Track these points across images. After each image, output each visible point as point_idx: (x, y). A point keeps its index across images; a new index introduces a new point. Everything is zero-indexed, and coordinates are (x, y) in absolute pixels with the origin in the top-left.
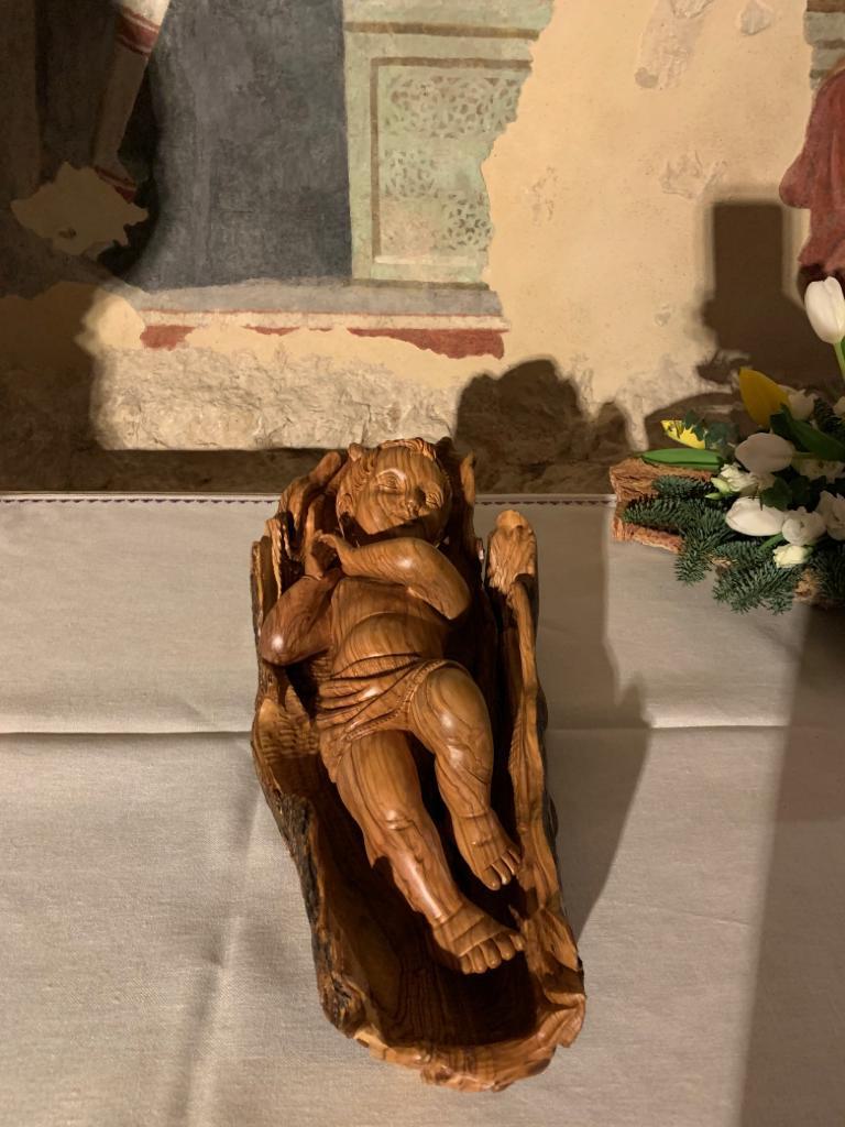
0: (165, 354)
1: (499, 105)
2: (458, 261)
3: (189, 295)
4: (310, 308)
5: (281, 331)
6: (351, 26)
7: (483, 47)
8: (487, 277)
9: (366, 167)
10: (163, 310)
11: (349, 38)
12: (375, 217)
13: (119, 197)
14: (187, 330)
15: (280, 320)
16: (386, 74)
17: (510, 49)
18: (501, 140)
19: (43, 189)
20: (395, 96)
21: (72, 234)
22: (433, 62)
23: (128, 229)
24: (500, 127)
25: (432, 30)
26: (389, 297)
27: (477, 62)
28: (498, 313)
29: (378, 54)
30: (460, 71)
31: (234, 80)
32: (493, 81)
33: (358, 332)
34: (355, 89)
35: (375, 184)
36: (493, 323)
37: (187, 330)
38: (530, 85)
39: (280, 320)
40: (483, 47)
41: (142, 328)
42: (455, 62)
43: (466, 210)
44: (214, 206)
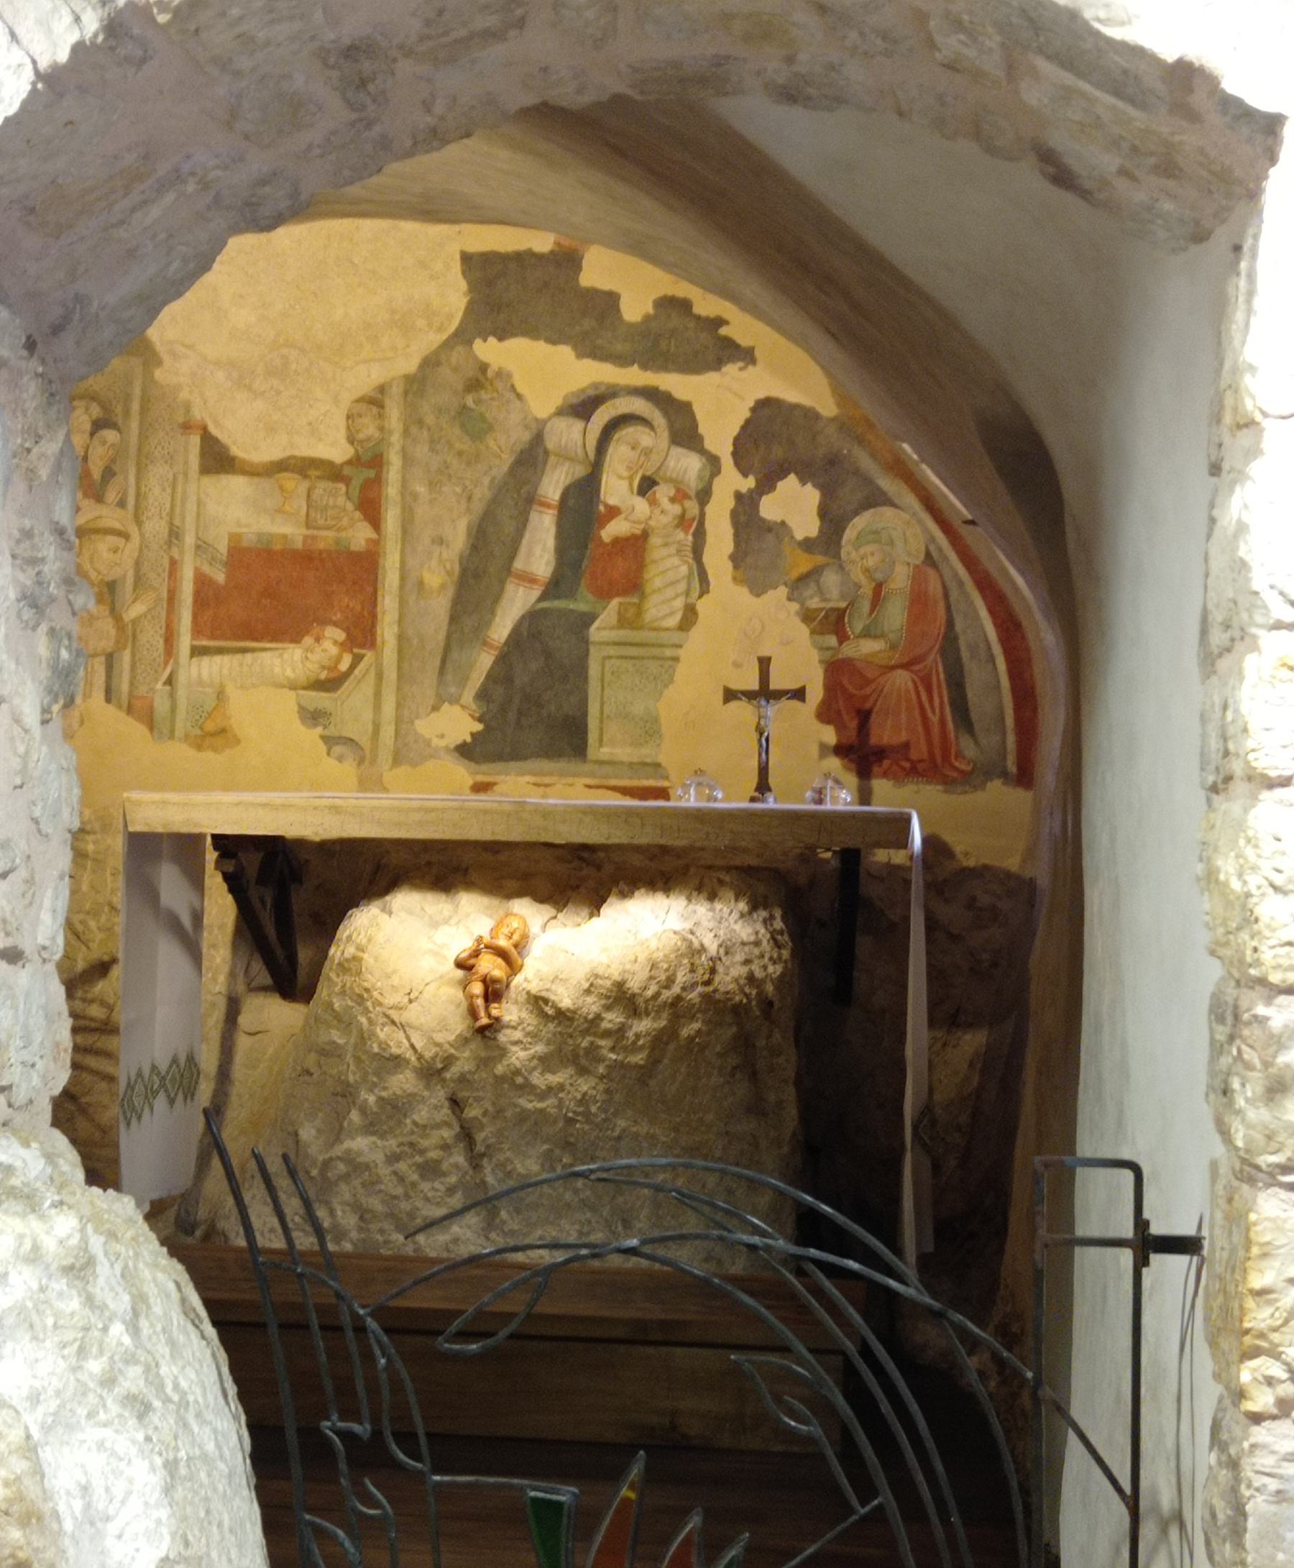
0: (482, 797)
3: (499, 766)
4: (562, 774)
5: (546, 786)
6: (592, 643)
7: (656, 651)
8: (661, 759)
9: (597, 705)
10: (484, 774)
11: (592, 650)
12: (601, 729)
13: (470, 719)
14: (495, 784)
15: (547, 780)
16: (608, 664)
18: (666, 692)
19: (432, 715)
20: (613, 673)
21: (442, 736)
22: (632, 658)
23: (472, 735)
24: (666, 686)
25: (631, 644)
27: (654, 658)
28: (667, 778)
29: (605, 654)
30: (646, 661)
31: (534, 666)
32: (661, 666)
33: (589, 787)
34: (594, 669)
35: (602, 713)
36: (665, 784)
37: (495, 784)
38: (681, 670)
39: (547, 780)
40: (656, 651)
41: (471, 782)
42: (643, 658)
43: (648, 725)
44: (518, 722)
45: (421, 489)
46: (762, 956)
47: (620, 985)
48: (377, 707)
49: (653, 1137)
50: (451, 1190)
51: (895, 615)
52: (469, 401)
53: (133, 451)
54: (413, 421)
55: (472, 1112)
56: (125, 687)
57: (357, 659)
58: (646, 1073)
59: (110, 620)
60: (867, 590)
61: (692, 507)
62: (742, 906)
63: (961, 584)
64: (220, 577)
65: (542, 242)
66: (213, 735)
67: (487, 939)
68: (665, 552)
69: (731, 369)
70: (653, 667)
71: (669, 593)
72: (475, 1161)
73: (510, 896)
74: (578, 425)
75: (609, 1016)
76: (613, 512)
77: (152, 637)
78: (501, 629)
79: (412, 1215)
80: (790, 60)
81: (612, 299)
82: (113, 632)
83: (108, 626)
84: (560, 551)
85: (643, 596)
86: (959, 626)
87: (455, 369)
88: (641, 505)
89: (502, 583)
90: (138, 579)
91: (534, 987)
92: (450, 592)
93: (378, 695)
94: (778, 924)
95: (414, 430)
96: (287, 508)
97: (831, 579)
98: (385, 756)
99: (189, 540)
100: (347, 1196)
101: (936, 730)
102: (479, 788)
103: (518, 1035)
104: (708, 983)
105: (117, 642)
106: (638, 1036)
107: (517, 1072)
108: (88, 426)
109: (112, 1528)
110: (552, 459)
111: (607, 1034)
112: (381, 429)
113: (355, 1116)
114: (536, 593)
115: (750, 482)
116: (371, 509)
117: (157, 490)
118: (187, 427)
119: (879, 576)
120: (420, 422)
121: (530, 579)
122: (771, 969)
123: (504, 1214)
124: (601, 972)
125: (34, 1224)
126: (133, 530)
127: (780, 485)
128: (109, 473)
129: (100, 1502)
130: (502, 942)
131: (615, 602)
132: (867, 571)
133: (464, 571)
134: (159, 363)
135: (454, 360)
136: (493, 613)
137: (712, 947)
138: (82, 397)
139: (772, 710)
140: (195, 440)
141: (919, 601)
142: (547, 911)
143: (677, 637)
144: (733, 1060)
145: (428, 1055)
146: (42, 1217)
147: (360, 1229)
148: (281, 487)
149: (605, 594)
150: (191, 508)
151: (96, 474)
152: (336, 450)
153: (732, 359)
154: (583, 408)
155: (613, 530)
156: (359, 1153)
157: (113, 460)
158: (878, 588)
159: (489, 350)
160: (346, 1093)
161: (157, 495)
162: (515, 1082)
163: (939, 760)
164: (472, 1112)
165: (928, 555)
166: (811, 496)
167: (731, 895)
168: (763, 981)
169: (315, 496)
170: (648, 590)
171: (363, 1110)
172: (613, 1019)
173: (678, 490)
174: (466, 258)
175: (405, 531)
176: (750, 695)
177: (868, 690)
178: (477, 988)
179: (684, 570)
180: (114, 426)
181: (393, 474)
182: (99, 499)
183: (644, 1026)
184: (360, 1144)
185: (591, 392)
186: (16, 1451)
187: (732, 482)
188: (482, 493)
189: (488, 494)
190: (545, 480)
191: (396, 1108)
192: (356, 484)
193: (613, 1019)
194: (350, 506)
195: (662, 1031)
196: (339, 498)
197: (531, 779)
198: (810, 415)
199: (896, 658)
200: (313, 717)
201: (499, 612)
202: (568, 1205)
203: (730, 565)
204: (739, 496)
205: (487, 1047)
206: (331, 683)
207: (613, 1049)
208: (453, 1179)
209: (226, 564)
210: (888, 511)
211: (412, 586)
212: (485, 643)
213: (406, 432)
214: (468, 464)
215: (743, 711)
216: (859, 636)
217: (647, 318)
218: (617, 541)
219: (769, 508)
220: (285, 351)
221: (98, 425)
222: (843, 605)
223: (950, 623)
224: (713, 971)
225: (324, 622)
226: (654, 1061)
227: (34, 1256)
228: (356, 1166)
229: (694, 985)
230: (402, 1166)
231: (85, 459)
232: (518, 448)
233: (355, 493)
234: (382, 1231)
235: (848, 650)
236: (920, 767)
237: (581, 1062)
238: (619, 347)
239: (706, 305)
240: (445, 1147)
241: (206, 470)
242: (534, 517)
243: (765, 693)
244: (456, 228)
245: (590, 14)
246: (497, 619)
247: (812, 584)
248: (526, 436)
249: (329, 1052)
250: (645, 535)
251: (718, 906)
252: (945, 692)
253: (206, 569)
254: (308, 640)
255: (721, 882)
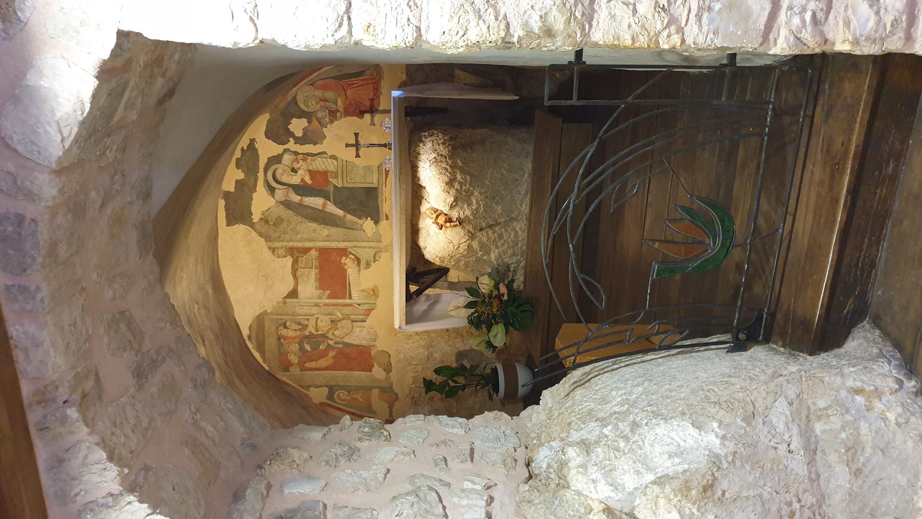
1: (352, 164)
2: (374, 170)
7: (344, 167)
15: (384, 199)
17: (344, 163)
21: (372, 229)
26: (380, 181)
31: (351, 203)
38: (349, 160)
39: (384, 199)
40: (344, 167)
45: (299, 236)
46: (437, 140)
47: (447, 184)
48: (365, 247)
49: (491, 173)
50: (506, 230)
51: (330, 95)
52: (271, 223)
53: (293, 317)
54: (279, 239)
55: (484, 225)
56: (361, 317)
57: (351, 253)
58: (472, 176)
59: (342, 321)
60: (322, 103)
61: (300, 157)
62: (421, 145)
63: (319, 74)
64: (328, 292)
65: (222, 203)
66: (374, 293)
67: (433, 220)
68: (314, 165)
69: (257, 146)
70: (349, 168)
71: (326, 163)
72: (498, 224)
73: (420, 212)
74: (277, 190)
75: (456, 187)
76: (303, 180)
77: (346, 310)
78: (340, 213)
79: (513, 241)
80: (131, 203)
81: (237, 181)
82: (346, 321)
83: (343, 322)
84: (315, 196)
85: (328, 171)
86: (332, 75)
87: (262, 227)
88: (300, 172)
89: (326, 212)
90: (330, 315)
91: (448, 208)
92: (329, 227)
93: (360, 247)
94: (426, 134)
95: (281, 239)
96: (307, 274)
97: (320, 115)
98: (379, 245)
99: (318, 301)
100: (508, 259)
101: (365, 82)
102: (387, 218)
103: (461, 212)
104: (445, 157)
105: (348, 319)
106: (462, 178)
107: (472, 213)
108: (286, 330)
109: (682, 444)
110: (288, 199)
111: (461, 187)
112: (282, 248)
113: (485, 258)
114: (329, 202)
115: (291, 139)
116: (306, 250)
117: (304, 310)
118: (285, 303)
119: (318, 100)
120: (279, 237)
121: (325, 204)
122: (440, 137)
123: (513, 216)
124: (443, 189)
125: (571, 464)
126: (316, 316)
127: (291, 130)
128: (299, 324)
129: (672, 448)
130: (434, 216)
131: (330, 179)
132: (317, 104)
133: (323, 224)
134: (266, 311)
135: (259, 228)
136: (336, 215)
137: (434, 155)
138: (277, 332)
139: (362, 141)
140: (288, 300)
141: (325, 88)
142: (424, 202)
143: (340, 161)
144: (469, 150)
145: (468, 238)
146: (569, 460)
147: (517, 256)
148: (301, 276)
149: (328, 182)
150: (307, 301)
151: (300, 327)
152: (289, 260)
153: (254, 145)
154: (272, 190)
155: (308, 180)
156: (495, 256)
157: (295, 322)
158: (321, 100)
159: (256, 218)
160: (478, 260)
161: (305, 310)
162: (475, 213)
163: (372, 81)
164: (484, 225)
165: (311, 85)
166: (294, 121)
167: (418, 148)
168: (444, 140)
169: (303, 266)
170: (326, 170)
171: (483, 255)
172: (457, 185)
173: (295, 161)
174: (228, 225)
175: (312, 241)
176: (357, 150)
177: (353, 103)
178: (448, 224)
179: (319, 159)
180: (285, 323)
181: (295, 244)
182: (307, 326)
183: (459, 177)
184: (493, 256)
185: (267, 187)
186: (662, 490)
187: (291, 145)
188: (299, 219)
189: (300, 217)
190: (294, 201)
191: (482, 246)
192: (298, 255)
193: (457, 185)
194: (305, 256)
195: (460, 171)
196: (303, 260)
197: (384, 203)
198: (269, 121)
199: (343, 94)
200: (368, 265)
201: (335, 213)
202: (511, 197)
203: (317, 145)
204: (295, 143)
205: (465, 221)
206: (358, 260)
207: (466, 186)
208: (503, 230)
209: (325, 291)
210: (298, 97)
211: (328, 238)
212: (344, 217)
213: (282, 241)
214: (291, 223)
215: (362, 151)
216: (337, 105)
217: (243, 171)
218: (311, 179)
219: (299, 133)
220: (260, 276)
221: (285, 327)
222: (327, 111)
223: (332, 78)
224: (442, 155)
225: (340, 263)
226: (469, 173)
227: (584, 466)
228: (499, 256)
229: (446, 162)
230: (499, 244)
231: (295, 330)
232: (285, 208)
233: (301, 255)
234: (518, 250)
235: (341, 109)
236: (376, 87)
237: (469, 194)
238: (252, 179)
239: (238, 154)
240: (494, 233)
241: (297, 297)
242: (305, 204)
243: (357, 145)
244: (219, 228)
245: (117, 286)
246: (337, 214)
247: (322, 120)
248: (281, 206)
249: (467, 265)
250: (309, 171)
251: (421, 152)
252: (353, 79)
253: (326, 296)
254: (346, 267)
255: (414, 151)
